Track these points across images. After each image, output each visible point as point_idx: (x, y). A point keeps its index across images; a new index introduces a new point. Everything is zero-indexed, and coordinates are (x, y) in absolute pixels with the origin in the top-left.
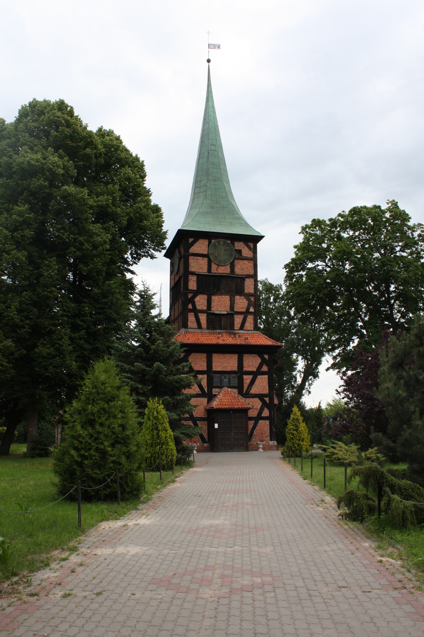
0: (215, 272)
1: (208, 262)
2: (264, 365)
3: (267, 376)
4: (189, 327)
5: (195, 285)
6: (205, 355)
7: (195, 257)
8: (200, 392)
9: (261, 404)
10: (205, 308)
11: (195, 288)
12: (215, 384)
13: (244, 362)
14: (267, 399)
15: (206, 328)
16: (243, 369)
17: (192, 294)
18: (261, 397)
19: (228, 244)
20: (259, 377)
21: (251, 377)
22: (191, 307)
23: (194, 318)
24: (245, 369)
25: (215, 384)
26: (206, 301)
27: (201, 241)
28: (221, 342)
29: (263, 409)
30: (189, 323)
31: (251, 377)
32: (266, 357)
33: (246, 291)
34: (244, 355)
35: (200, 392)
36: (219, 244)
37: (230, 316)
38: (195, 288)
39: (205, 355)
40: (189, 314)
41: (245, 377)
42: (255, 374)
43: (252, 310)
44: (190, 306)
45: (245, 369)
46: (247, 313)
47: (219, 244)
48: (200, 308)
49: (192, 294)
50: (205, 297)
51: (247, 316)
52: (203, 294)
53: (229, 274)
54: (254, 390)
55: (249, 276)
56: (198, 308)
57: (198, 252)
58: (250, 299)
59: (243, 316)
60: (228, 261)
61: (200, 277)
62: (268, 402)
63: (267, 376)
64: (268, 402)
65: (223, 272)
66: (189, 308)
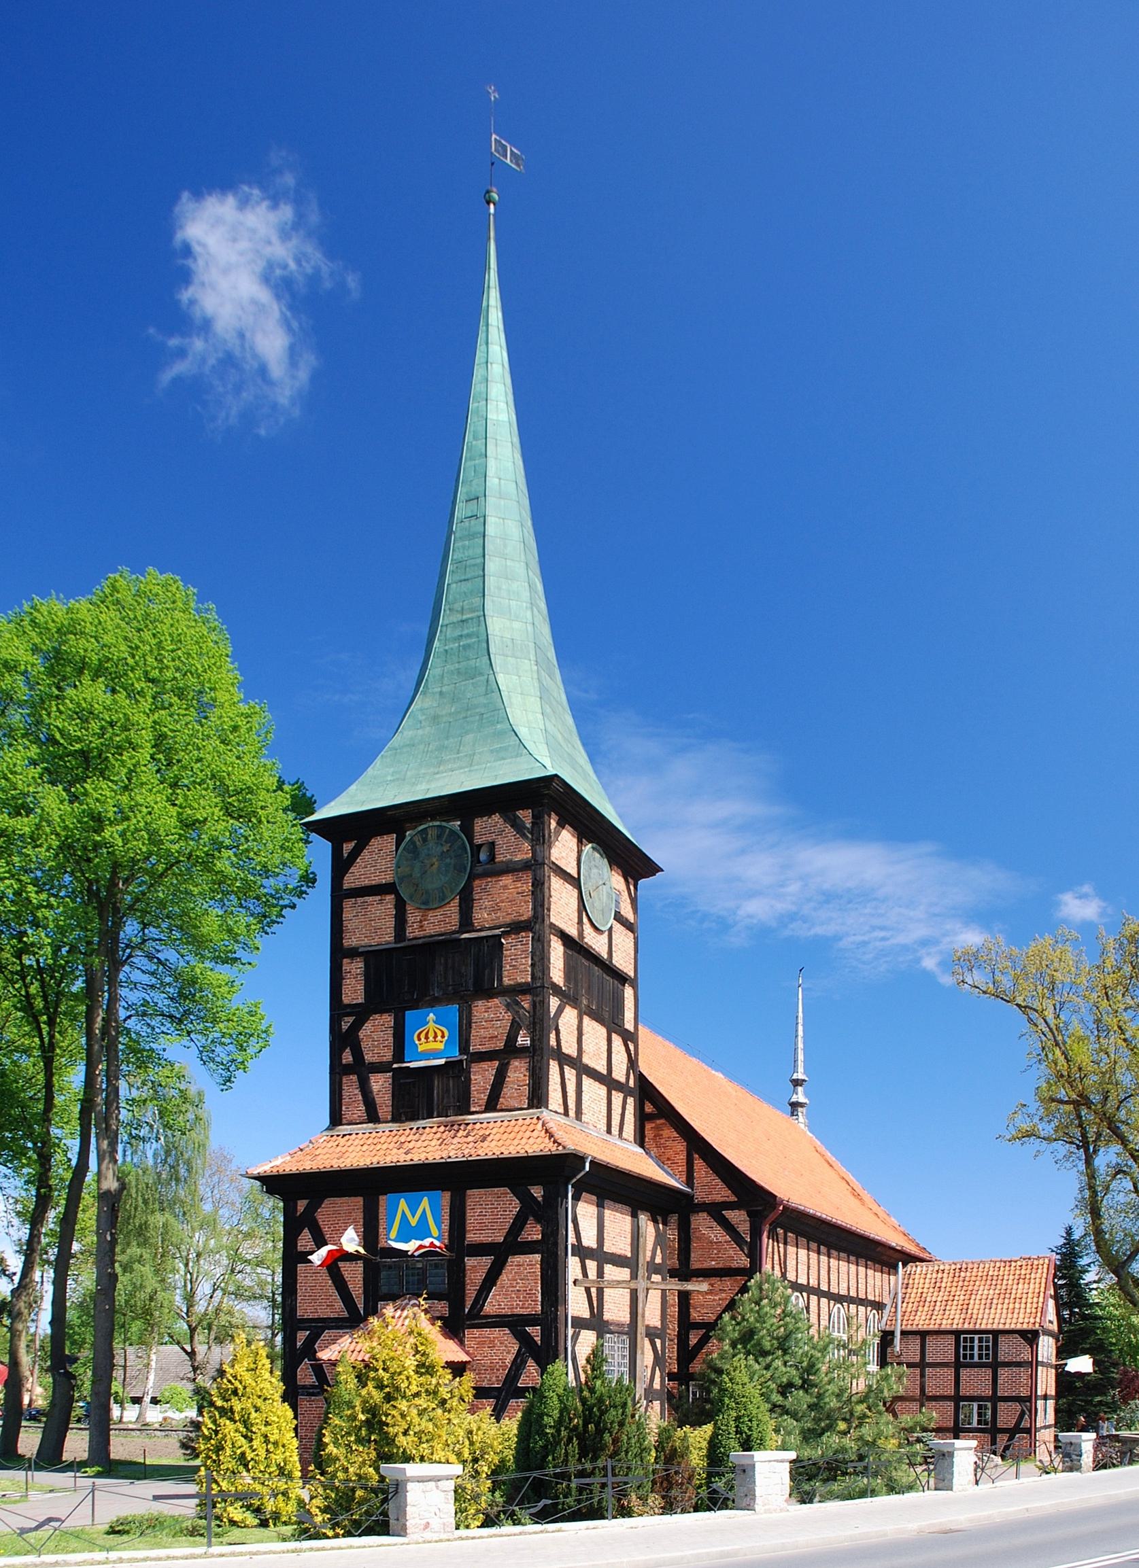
0: (417, 934)
1: (396, 907)
2: (531, 1220)
3: (538, 1257)
4: (344, 1121)
5: (361, 987)
6: (359, 1201)
7: (360, 900)
8: (346, 1314)
9: (516, 1347)
10: (388, 1055)
11: (361, 1000)
12: (384, 1290)
13: (469, 1213)
14: (535, 1332)
15: (389, 1117)
16: (464, 1238)
17: (351, 1019)
18: (515, 1323)
19: (452, 832)
20: (515, 1260)
21: (487, 1261)
22: (351, 1059)
23: (357, 1091)
24: (472, 1237)
25: (384, 1290)
26: (391, 1031)
27: (376, 843)
28: (418, 1157)
29: (524, 1362)
30: (344, 1108)
31: (487, 1261)
32: (537, 1192)
33: (506, 981)
34: (469, 1192)
35: (346, 1314)
36: (425, 840)
37: (456, 1072)
38: (361, 1000)
39: (359, 1201)
40: (344, 1080)
41: (470, 1262)
42: (500, 1253)
43: (523, 1040)
44: (347, 1057)
45: (472, 1237)
46: (510, 1050)
47: (425, 840)
48: (375, 1059)
49: (351, 1019)
50: (388, 1020)
51: (508, 1063)
52: (382, 1012)
53: (454, 932)
54: (495, 1304)
55: (516, 928)
56: (369, 1057)
57: (367, 883)
58: (518, 1003)
59: (497, 1063)
60: (452, 892)
61: (375, 959)
62: (538, 1339)
63: (538, 1257)
64: (538, 1339)
65: (438, 930)
66: (344, 1061)
